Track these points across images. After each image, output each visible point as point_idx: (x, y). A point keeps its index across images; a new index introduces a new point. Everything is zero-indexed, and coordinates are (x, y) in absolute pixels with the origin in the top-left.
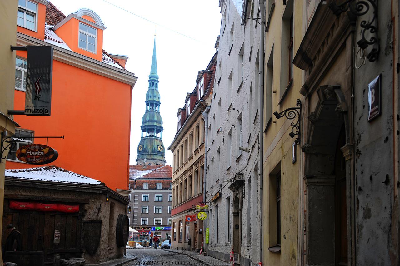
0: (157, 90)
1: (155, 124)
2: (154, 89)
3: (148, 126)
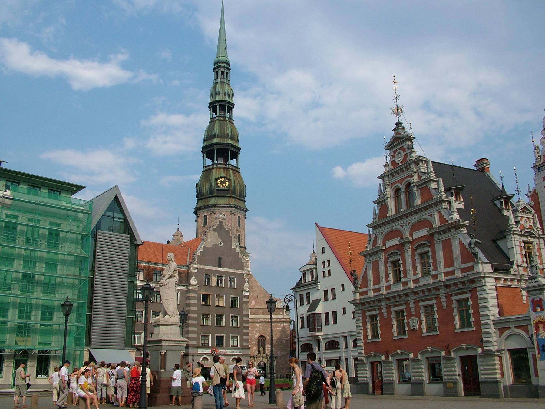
0: (228, 84)
1: (230, 141)
2: (224, 82)
3: (217, 144)
